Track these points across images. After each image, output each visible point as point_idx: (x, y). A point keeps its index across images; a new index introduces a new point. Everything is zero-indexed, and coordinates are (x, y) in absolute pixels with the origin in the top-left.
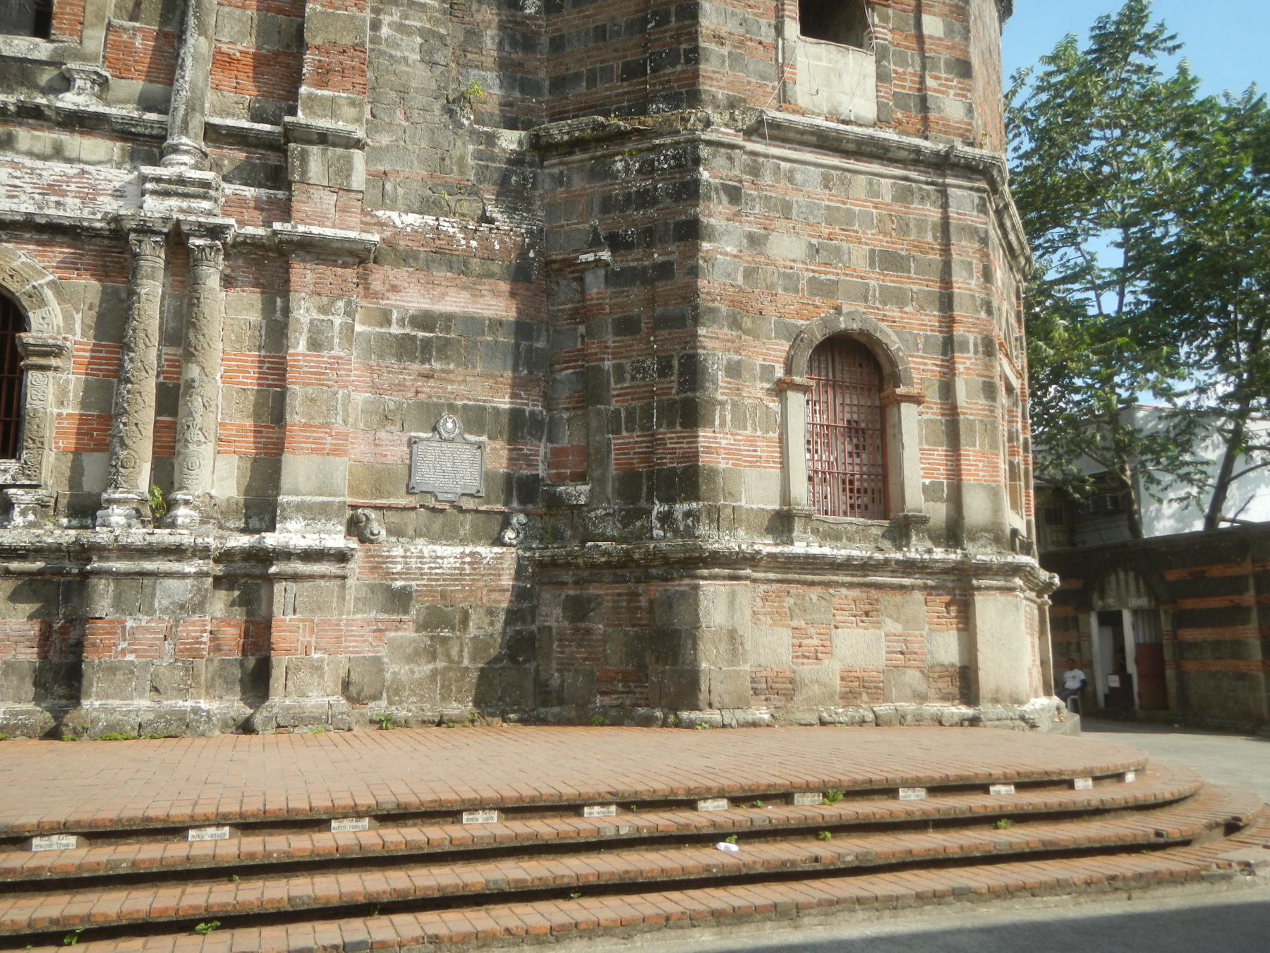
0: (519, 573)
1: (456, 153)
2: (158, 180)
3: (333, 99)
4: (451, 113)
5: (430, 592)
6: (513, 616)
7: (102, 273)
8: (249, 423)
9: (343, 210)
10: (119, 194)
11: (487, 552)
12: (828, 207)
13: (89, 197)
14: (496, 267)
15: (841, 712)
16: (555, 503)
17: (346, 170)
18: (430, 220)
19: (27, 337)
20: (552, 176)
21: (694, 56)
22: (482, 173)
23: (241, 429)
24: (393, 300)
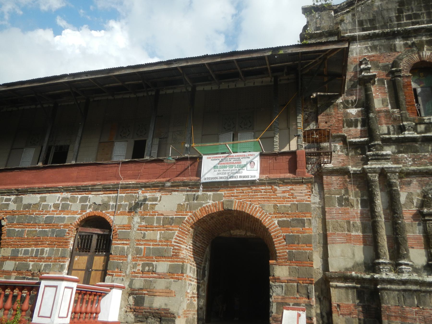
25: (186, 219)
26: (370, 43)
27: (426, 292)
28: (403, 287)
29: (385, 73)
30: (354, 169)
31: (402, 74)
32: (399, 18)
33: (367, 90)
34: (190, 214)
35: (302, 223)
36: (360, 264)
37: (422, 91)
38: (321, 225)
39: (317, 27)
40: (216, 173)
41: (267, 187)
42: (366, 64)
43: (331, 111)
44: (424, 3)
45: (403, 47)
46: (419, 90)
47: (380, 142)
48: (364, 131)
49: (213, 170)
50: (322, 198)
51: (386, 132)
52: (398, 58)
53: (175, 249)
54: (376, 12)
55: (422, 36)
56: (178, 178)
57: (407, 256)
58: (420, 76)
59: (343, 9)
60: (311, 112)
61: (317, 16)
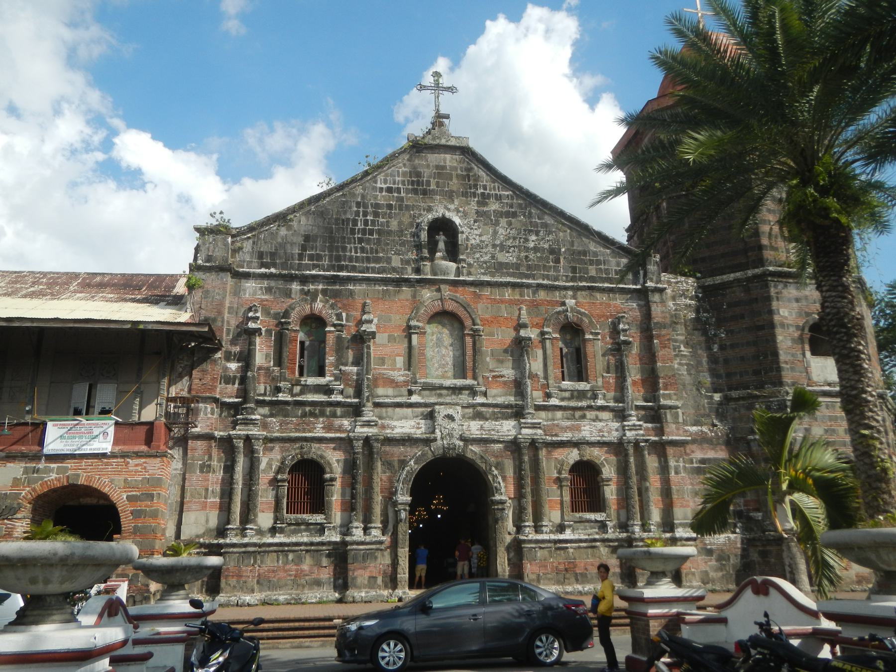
0: (742, 543)
1: (702, 404)
2: (628, 426)
3: (669, 394)
4: (698, 390)
5: (718, 549)
6: (743, 556)
7: (616, 455)
8: (660, 498)
9: (678, 429)
10: (617, 430)
11: (732, 536)
12: (829, 416)
13: (609, 432)
14: (721, 441)
15: (857, 587)
16: (750, 519)
17: (676, 416)
18: (699, 428)
19: (604, 476)
20: (732, 408)
21: (779, 369)
22: (710, 408)
23: (658, 500)
24: (693, 456)
25: (23, 494)
26: (266, 283)
27: (264, 552)
28: (243, 549)
29: (275, 322)
30: (221, 433)
31: (290, 327)
32: (301, 256)
33: (251, 343)
34: (28, 489)
35: (151, 497)
36: (213, 530)
37: (310, 345)
38: (179, 493)
39: (208, 256)
40: (63, 444)
41: (119, 460)
42: (256, 311)
43: (207, 366)
44: (329, 242)
45: (298, 293)
46: (307, 343)
47: (252, 405)
48: (241, 389)
49: (59, 440)
50: (185, 464)
51: (262, 392)
52: (290, 306)
53: (8, 528)
54: (280, 244)
55: (319, 282)
56: (15, 447)
57: (254, 521)
58: (311, 328)
59: (244, 234)
60: (186, 365)
61: (211, 240)
